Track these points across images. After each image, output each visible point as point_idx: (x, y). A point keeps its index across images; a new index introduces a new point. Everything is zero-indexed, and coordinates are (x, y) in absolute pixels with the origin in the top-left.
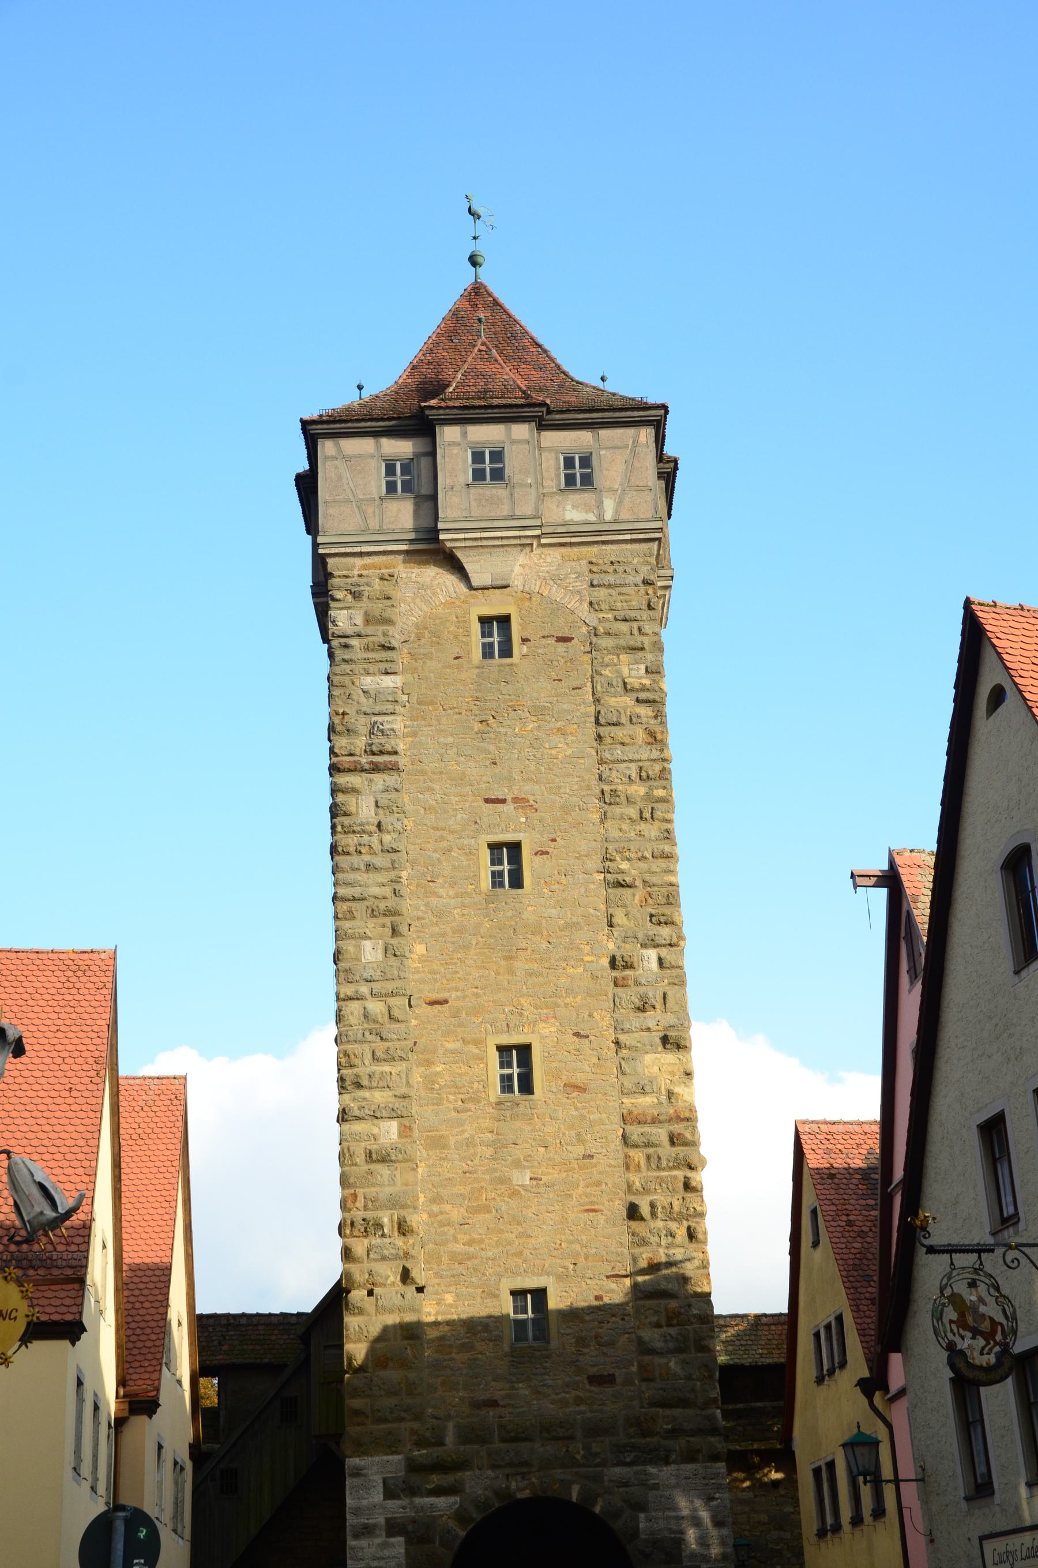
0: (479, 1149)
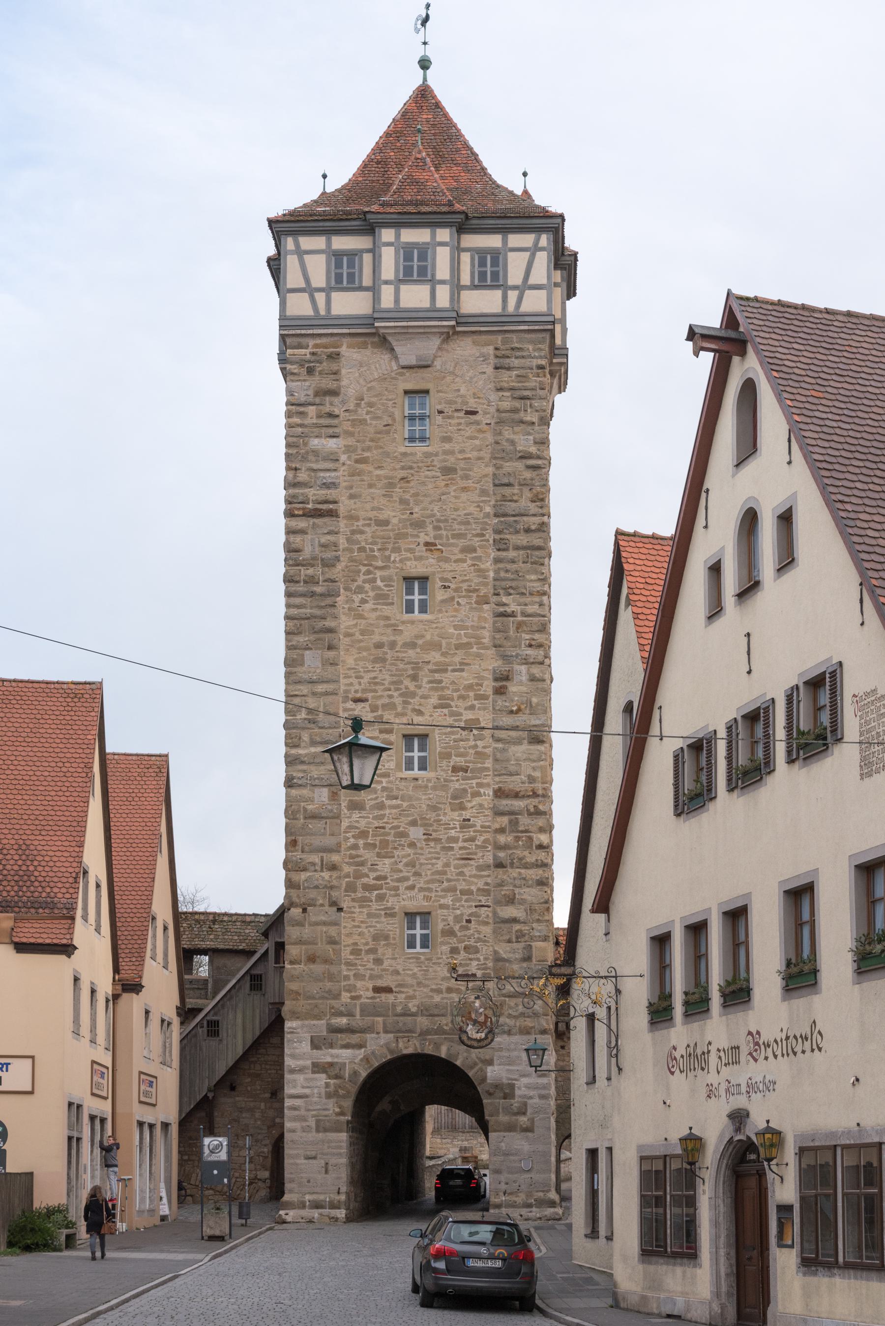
0: (387, 812)
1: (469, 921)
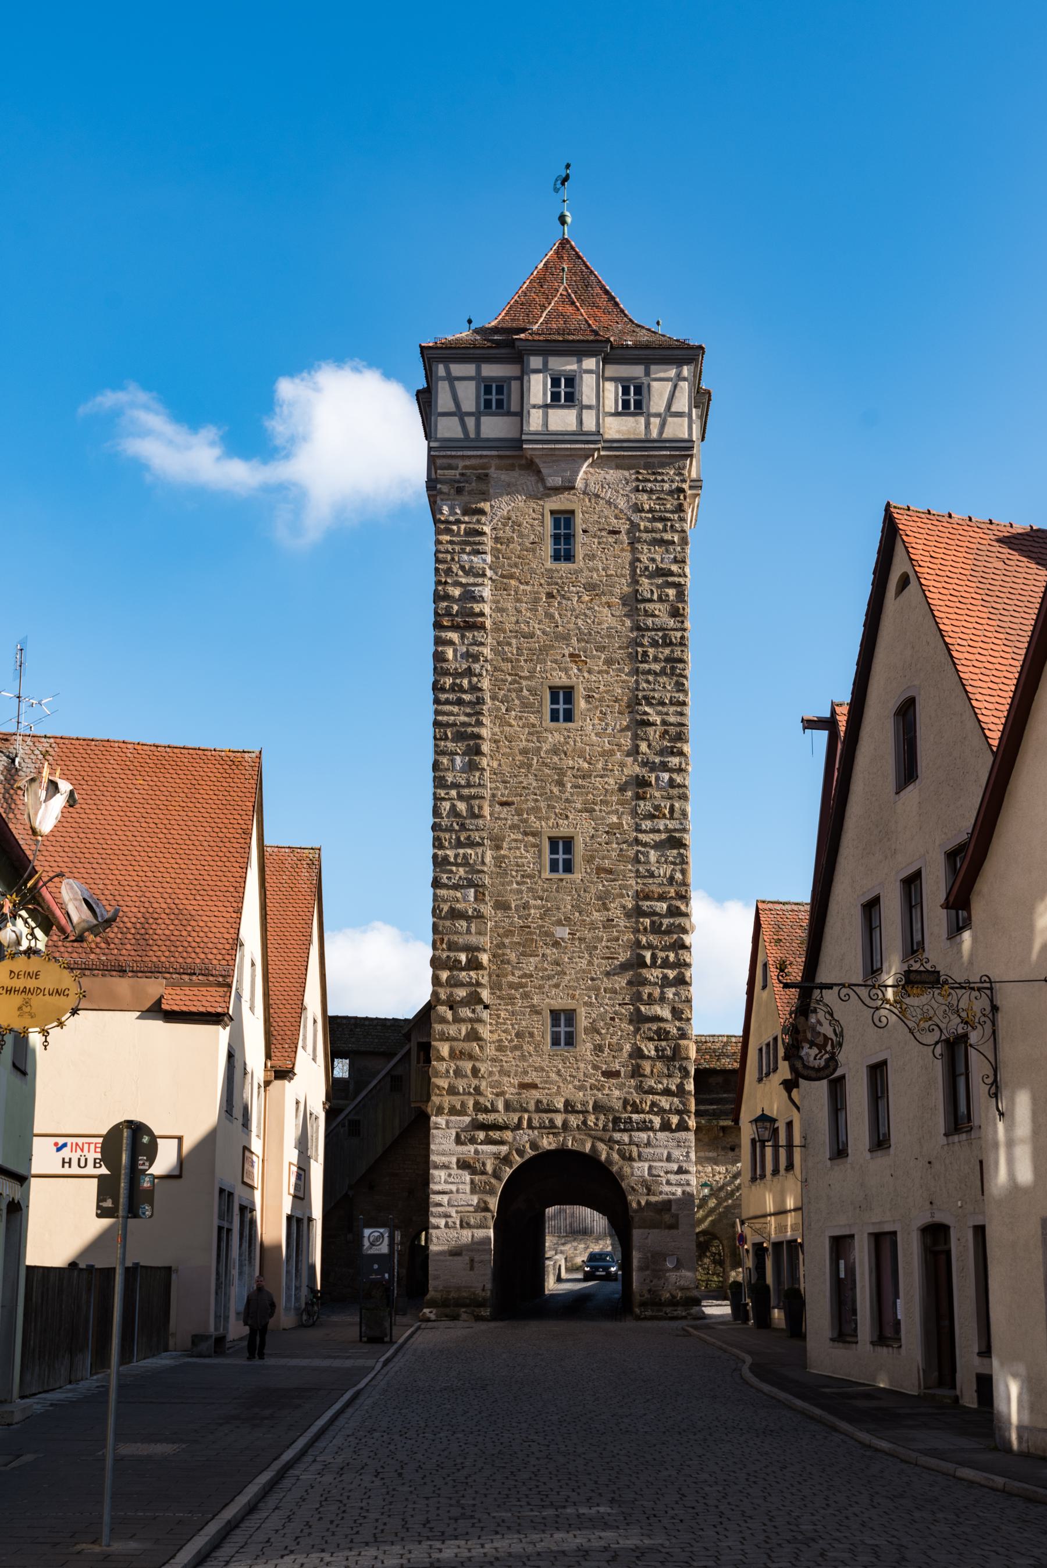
1: (613, 1019)
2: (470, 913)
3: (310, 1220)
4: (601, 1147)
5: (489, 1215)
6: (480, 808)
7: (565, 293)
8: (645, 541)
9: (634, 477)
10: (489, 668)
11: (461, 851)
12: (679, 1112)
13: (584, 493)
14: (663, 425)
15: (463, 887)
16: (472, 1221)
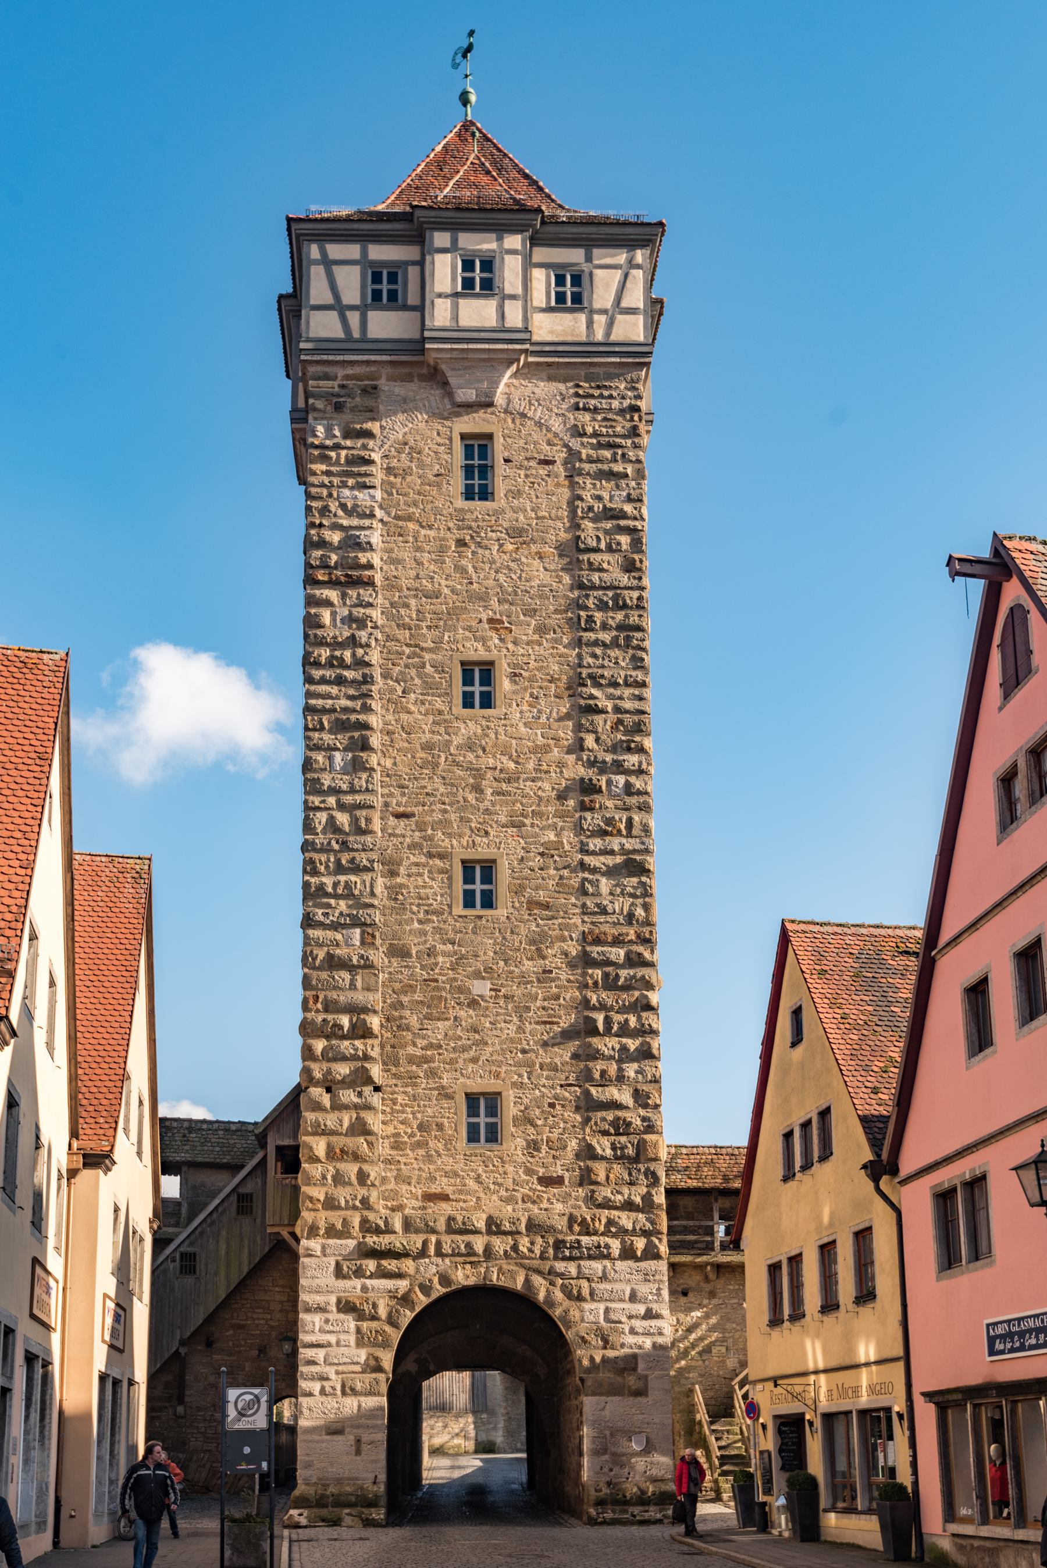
1: (552, 1105)
2: (355, 961)
3: (131, 1383)
4: (538, 1280)
5: (381, 1377)
6: (368, 820)
7: (477, 162)
8: (588, 474)
9: (572, 391)
10: (380, 636)
11: (342, 878)
12: (645, 1233)
13: (506, 411)
14: (610, 324)
15: (344, 926)
16: (359, 1386)
